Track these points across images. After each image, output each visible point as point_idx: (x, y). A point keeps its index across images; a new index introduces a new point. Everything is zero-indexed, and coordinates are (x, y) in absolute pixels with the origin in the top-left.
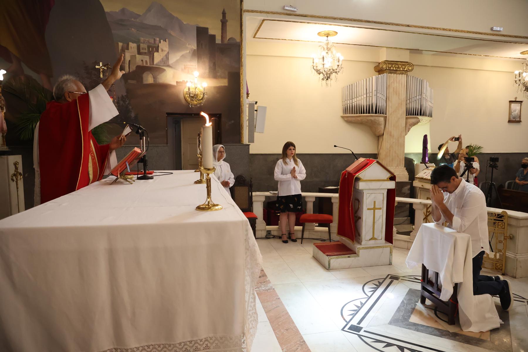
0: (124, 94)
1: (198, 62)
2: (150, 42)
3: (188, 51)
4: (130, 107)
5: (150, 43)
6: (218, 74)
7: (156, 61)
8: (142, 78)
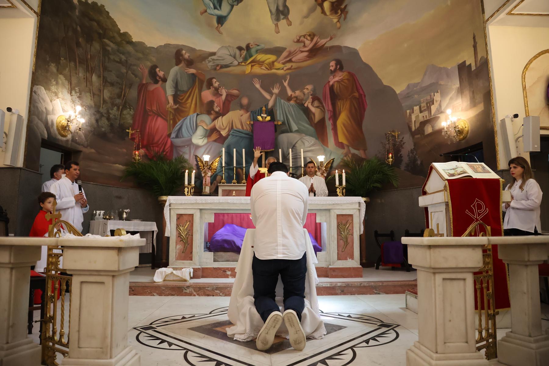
0: (413, 147)
1: (462, 97)
2: (428, 99)
3: (454, 92)
4: (417, 157)
5: (428, 100)
6: (477, 101)
7: (433, 113)
8: (424, 131)
